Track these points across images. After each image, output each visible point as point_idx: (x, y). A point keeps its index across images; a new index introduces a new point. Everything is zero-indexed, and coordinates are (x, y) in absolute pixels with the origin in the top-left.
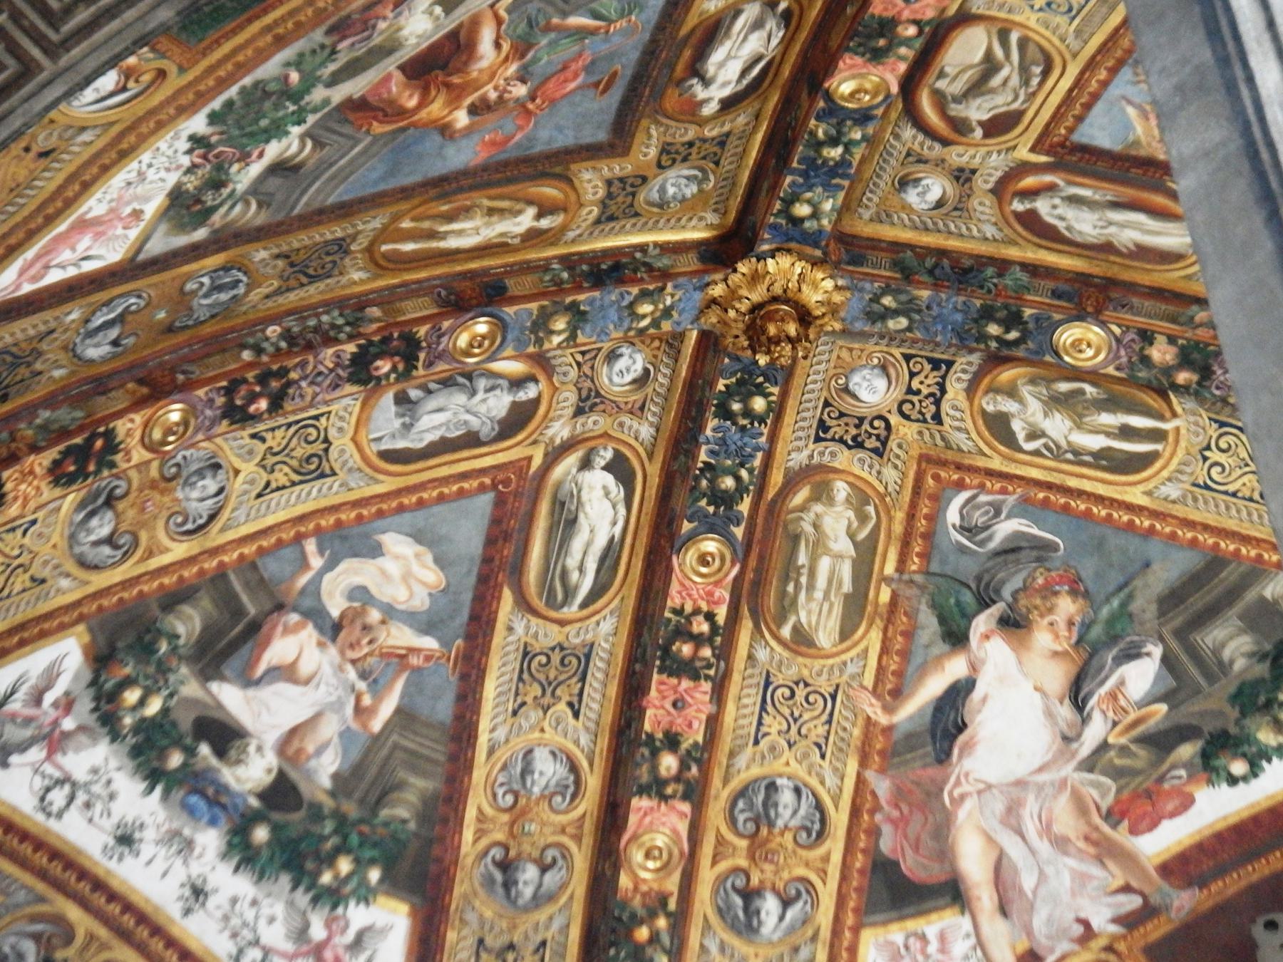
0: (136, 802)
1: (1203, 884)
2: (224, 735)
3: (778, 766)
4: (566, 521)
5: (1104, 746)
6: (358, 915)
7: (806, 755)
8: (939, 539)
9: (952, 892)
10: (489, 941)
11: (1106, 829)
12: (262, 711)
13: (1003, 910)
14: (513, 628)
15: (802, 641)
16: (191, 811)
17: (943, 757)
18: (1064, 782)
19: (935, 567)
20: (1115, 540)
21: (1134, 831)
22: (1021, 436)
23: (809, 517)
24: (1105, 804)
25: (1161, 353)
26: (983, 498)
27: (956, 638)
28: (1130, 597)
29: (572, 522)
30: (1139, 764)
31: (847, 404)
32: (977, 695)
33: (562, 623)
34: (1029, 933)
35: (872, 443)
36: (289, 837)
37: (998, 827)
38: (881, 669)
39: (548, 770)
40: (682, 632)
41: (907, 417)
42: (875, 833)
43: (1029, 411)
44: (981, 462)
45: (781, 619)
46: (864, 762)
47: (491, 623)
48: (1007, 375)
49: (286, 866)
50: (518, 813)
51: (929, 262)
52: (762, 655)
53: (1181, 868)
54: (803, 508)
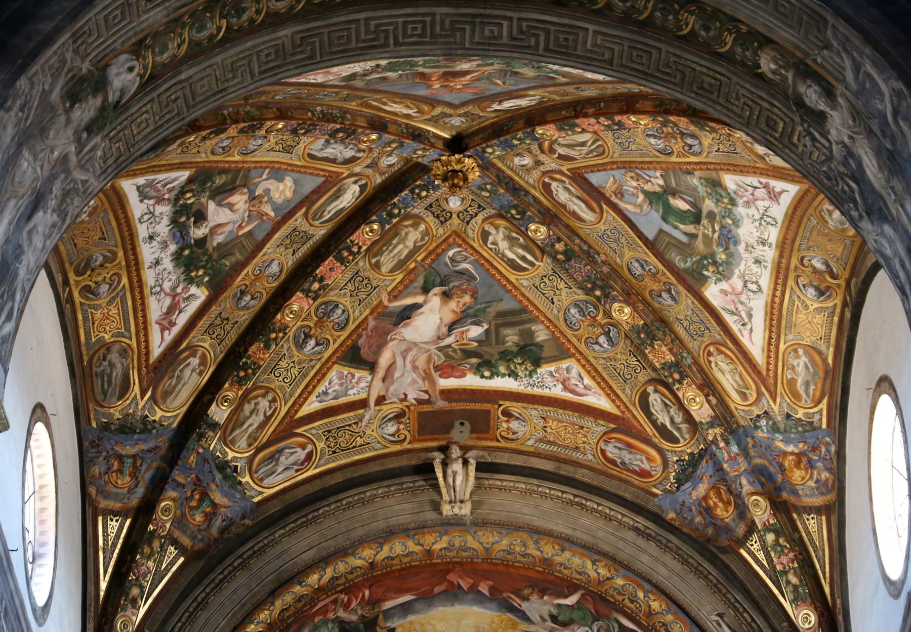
0: (163, 228)
1: (450, 401)
2: (200, 217)
3: (343, 300)
4: (336, 196)
5: (449, 346)
6: (193, 290)
7: (354, 302)
8: (441, 258)
9: (372, 367)
10: (223, 315)
11: (432, 371)
12: (216, 214)
13: (384, 380)
14: (298, 221)
15: (377, 266)
16: (174, 236)
17: (396, 324)
18: (429, 350)
19: (434, 265)
20: (497, 287)
21: (441, 376)
22: (490, 242)
23: (406, 230)
24: (438, 363)
25: (559, 247)
26: (464, 253)
27: (426, 290)
28: (489, 307)
29: (338, 197)
30: (457, 357)
31: (444, 204)
32: (420, 311)
33: (311, 225)
34: (387, 390)
35: (442, 219)
36: (191, 258)
37: (399, 353)
38: (395, 287)
39: (275, 268)
40: (348, 249)
41: (459, 217)
42: (360, 336)
43: (499, 237)
44: (471, 242)
45: (374, 257)
46: (371, 313)
47: (294, 215)
48: (499, 222)
49: (186, 266)
50: (257, 278)
51: (507, 180)
52: (361, 264)
53: (447, 394)
54: (406, 227)
